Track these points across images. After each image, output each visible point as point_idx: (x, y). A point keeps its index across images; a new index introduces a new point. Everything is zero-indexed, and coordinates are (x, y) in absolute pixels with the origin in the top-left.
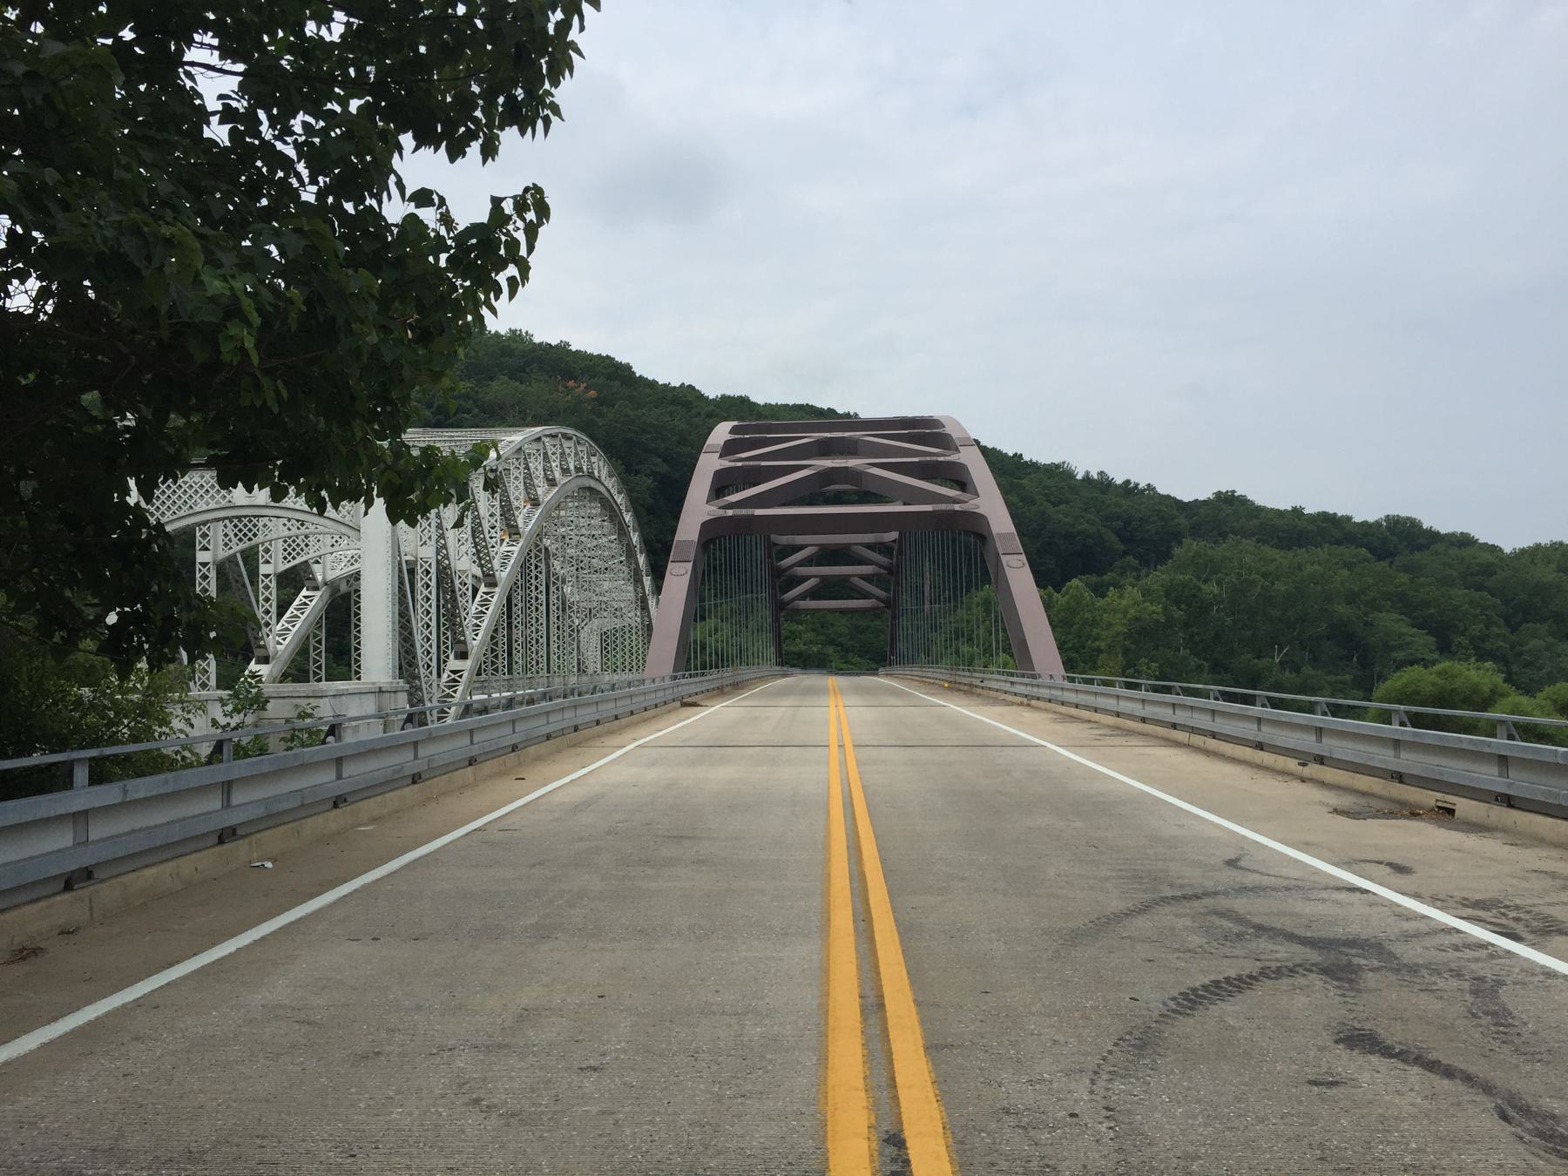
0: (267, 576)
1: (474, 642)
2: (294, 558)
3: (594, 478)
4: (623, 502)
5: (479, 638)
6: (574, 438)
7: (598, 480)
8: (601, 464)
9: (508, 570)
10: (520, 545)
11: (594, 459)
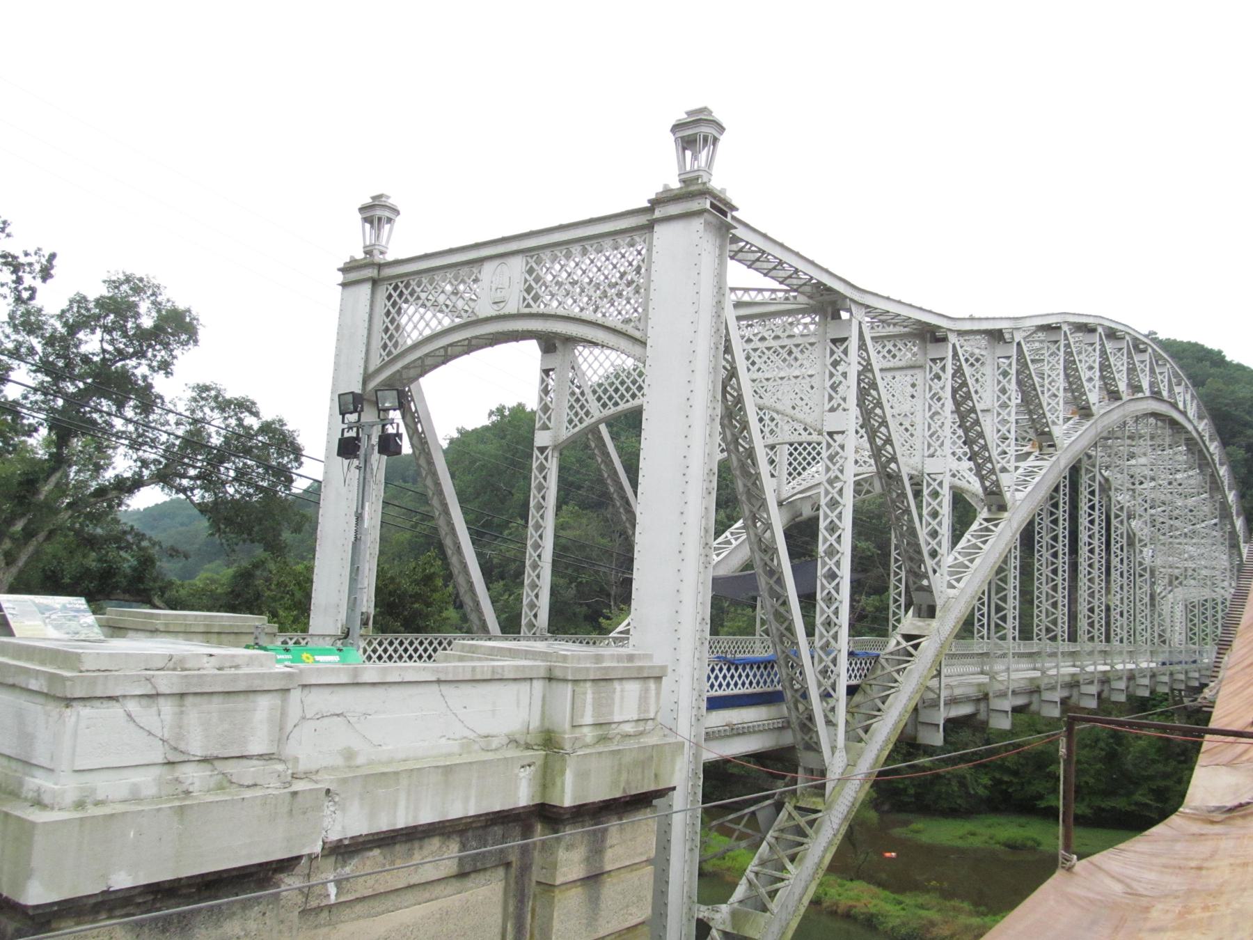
1: (951, 592)
4: (1217, 451)
5: (961, 585)
7: (1184, 413)
8: (1188, 397)
9: (1029, 489)
10: (1054, 459)
11: (1177, 389)
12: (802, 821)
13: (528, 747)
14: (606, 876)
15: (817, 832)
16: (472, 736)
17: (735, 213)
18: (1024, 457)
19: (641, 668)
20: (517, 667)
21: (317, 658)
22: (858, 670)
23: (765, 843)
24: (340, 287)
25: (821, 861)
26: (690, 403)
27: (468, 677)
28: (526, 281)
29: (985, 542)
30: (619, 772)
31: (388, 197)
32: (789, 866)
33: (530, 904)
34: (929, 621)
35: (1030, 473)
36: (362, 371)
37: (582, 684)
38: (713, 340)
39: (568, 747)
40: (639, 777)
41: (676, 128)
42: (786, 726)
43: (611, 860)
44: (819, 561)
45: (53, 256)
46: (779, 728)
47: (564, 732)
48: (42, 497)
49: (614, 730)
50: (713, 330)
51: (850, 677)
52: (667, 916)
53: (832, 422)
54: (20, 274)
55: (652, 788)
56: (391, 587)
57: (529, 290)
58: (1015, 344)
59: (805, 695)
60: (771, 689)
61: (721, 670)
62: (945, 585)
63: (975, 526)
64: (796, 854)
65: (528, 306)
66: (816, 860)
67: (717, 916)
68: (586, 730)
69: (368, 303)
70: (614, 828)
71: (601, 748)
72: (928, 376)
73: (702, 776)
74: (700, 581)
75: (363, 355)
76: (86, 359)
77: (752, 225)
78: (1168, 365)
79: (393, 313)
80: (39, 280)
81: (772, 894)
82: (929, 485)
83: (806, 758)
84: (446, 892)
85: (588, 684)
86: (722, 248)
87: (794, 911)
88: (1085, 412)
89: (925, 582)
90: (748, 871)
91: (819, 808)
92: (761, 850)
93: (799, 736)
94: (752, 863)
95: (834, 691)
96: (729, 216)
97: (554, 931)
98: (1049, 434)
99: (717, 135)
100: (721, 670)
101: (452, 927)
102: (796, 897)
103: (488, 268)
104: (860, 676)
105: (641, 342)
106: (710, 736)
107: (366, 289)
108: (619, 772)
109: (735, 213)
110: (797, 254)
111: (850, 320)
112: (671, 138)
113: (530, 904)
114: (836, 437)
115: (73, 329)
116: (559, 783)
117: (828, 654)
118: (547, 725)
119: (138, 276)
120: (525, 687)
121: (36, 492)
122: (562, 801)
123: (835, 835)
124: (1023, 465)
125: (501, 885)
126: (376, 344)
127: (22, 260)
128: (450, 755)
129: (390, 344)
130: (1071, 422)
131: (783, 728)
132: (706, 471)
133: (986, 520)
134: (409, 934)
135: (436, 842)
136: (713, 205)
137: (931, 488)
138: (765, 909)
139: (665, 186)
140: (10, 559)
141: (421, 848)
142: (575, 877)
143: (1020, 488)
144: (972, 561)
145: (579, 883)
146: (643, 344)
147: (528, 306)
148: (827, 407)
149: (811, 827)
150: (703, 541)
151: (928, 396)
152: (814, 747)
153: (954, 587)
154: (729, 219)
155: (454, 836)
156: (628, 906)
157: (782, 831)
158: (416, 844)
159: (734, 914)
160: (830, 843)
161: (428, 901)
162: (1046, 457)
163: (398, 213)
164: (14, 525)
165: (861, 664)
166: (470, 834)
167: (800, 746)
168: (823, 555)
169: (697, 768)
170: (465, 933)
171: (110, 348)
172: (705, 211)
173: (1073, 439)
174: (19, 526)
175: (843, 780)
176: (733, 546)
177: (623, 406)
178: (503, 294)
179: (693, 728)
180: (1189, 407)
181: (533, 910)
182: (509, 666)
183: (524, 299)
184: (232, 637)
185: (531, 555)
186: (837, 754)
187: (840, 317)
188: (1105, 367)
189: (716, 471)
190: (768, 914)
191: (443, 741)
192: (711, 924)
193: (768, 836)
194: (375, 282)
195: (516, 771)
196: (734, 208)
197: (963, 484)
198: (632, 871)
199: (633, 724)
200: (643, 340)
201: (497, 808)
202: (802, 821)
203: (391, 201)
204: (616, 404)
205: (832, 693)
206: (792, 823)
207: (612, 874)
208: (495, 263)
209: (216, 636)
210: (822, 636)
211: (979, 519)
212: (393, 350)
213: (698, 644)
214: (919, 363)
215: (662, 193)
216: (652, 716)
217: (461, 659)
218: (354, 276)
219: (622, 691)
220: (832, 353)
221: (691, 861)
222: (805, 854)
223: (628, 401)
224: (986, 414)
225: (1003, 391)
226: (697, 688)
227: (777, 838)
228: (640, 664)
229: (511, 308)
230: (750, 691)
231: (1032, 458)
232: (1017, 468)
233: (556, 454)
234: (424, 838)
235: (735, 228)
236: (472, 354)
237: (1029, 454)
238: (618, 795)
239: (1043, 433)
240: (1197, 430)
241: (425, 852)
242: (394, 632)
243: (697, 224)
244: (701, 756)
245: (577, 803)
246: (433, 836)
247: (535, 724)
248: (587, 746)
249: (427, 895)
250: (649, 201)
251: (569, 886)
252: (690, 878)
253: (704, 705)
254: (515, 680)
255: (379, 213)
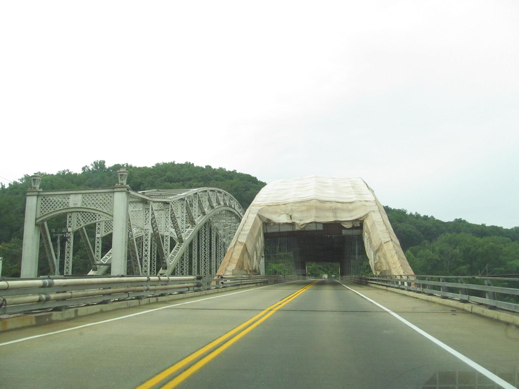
0: (98, 238)
1: (170, 263)
2: (108, 231)
3: (232, 208)
6: (223, 193)
7: (234, 209)
8: (235, 203)
9: (189, 237)
10: (195, 228)
11: (231, 201)
18: (188, 227)
28: (82, 200)
29: (178, 251)
34: (166, 270)
35: (189, 232)
36: (35, 217)
57: (83, 202)
58: (185, 201)
62: (169, 262)
63: (176, 247)
65: (83, 206)
69: (36, 201)
72: (165, 212)
75: (35, 213)
78: (229, 196)
82: (165, 238)
86: (128, 196)
88: (204, 214)
89: (165, 261)
98: (194, 221)
105: (112, 216)
114: (146, 230)
124: (188, 230)
126: (39, 211)
129: (43, 211)
130: (200, 216)
133: (179, 245)
136: (127, 189)
137: (166, 239)
143: (186, 236)
144: (175, 256)
146: (113, 216)
147: (83, 206)
148: (145, 224)
151: (165, 217)
153: (171, 262)
162: (193, 227)
173: (200, 222)
177: (92, 222)
178: (76, 202)
180: (235, 206)
188: (209, 200)
194: (38, 196)
197: (173, 236)
204: (90, 221)
208: (74, 195)
211: (177, 245)
212: (44, 213)
214: (163, 209)
220: (146, 212)
223: (94, 221)
224: (178, 218)
225: (183, 212)
229: (79, 206)
231: (190, 228)
232: (186, 231)
233: (73, 233)
237: (189, 226)
239: (193, 221)
240: (238, 213)
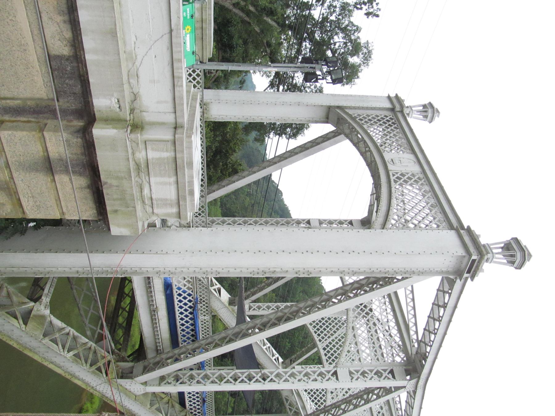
12: (101, 364)
13: (132, 111)
14: (52, 178)
15: (93, 372)
16: (137, 63)
17: (469, 279)
19: (185, 199)
20: (182, 98)
21: (188, 36)
22: (195, 407)
23: (87, 340)
24: (387, 96)
25: (76, 378)
26: (352, 253)
27: (175, 56)
30: (117, 178)
31: (438, 116)
32: (72, 353)
33: (33, 120)
37: (173, 148)
38: (390, 270)
39: (133, 136)
40: (115, 196)
41: (516, 240)
42: (158, 351)
43: (62, 179)
44: (259, 370)
45: (377, 16)
46: (157, 347)
47: (141, 135)
48: (265, 18)
49: (143, 175)
50: (396, 270)
51: (189, 393)
52: (36, 253)
53: (342, 373)
54: (368, 4)
55: (109, 208)
56: (230, 152)
59: (177, 360)
60: (180, 340)
61: (190, 301)
64: (80, 358)
65: (394, 175)
66: (77, 374)
67: (42, 307)
68: (144, 153)
70: (81, 181)
71: (132, 164)
73: (123, 276)
74: (243, 270)
76: (331, 37)
77: (462, 295)
79: (379, 121)
80: (366, 12)
81: (55, 341)
83: (140, 366)
84: (38, 48)
85: (173, 154)
87: (44, 358)
90: (70, 328)
91: (109, 375)
92: (83, 337)
93: (152, 361)
94: (75, 332)
95: (181, 383)
96: (468, 275)
97: (15, 132)
99: (515, 265)
100: (190, 301)
101: (16, 55)
102: (54, 359)
103: (412, 157)
104: (191, 409)
106: (148, 281)
107: (389, 105)
108: (117, 178)
109: (469, 279)
110: (445, 334)
111: (406, 380)
112: (509, 239)
113: (33, 120)
115: (344, 30)
116: (107, 126)
117: (203, 378)
118: (146, 127)
119: (372, 56)
120: (169, 107)
121: (267, 16)
122: (95, 128)
123: (93, 387)
125: (44, 96)
127: (374, 4)
128: (125, 43)
131: (157, 350)
132: (310, 270)
134: (10, 18)
135: (68, 34)
136: (474, 261)
138: (45, 335)
139: (480, 235)
140: (236, 5)
141: (65, 22)
142: (49, 149)
145: (46, 154)
147: (394, 175)
148: (352, 370)
149: (96, 369)
150: (267, 270)
152: (146, 370)
154: (466, 275)
155: (73, 51)
156: (33, 197)
157: (95, 352)
158: (66, 18)
159: (43, 317)
160: (87, 384)
161: (32, 34)
163: (430, 122)
164: (252, 6)
165: (199, 409)
166: (75, 64)
167: (146, 363)
168: (263, 372)
169: (128, 273)
170: (12, 66)
171: (337, 46)
172: (470, 255)
174: (252, 8)
175: (128, 393)
176: (262, 347)
179: (151, 269)
181: (29, 122)
182: (183, 91)
183: (397, 173)
184: (200, 35)
185: (251, 220)
186: (142, 387)
187: (407, 376)
189: (311, 276)
190: (42, 337)
191: (134, 39)
192: (37, 303)
193: (91, 343)
194: (393, 110)
195: (115, 95)
196: (472, 278)
198: (56, 200)
199: (149, 196)
200: (387, 226)
201: (91, 80)
202: (101, 364)
203: (436, 119)
205: (179, 382)
206: (99, 358)
207: (54, 183)
208: (415, 160)
209: (201, 26)
210: (213, 374)
213: (204, 270)
215: (476, 235)
216: (156, 211)
217: (188, 92)
218: (395, 101)
219: (170, 184)
221: (71, 273)
222: (79, 364)
226: (177, 271)
227: (90, 348)
228: (187, 198)
229: (390, 167)
230: (178, 324)
234: (71, 24)
235: (461, 281)
236: (361, 156)
238: (103, 177)
241: (62, 25)
242: (206, 152)
243: (461, 252)
244: (135, 275)
245: (95, 141)
246: (73, 33)
247: (148, 117)
248: (133, 154)
249: (36, 32)
250: (469, 227)
251: (44, 145)
252: (60, 272)
253: (166, 276)
254: (174, 99)
255: (430, 110)
